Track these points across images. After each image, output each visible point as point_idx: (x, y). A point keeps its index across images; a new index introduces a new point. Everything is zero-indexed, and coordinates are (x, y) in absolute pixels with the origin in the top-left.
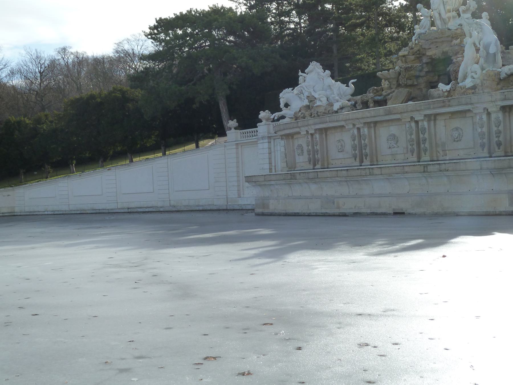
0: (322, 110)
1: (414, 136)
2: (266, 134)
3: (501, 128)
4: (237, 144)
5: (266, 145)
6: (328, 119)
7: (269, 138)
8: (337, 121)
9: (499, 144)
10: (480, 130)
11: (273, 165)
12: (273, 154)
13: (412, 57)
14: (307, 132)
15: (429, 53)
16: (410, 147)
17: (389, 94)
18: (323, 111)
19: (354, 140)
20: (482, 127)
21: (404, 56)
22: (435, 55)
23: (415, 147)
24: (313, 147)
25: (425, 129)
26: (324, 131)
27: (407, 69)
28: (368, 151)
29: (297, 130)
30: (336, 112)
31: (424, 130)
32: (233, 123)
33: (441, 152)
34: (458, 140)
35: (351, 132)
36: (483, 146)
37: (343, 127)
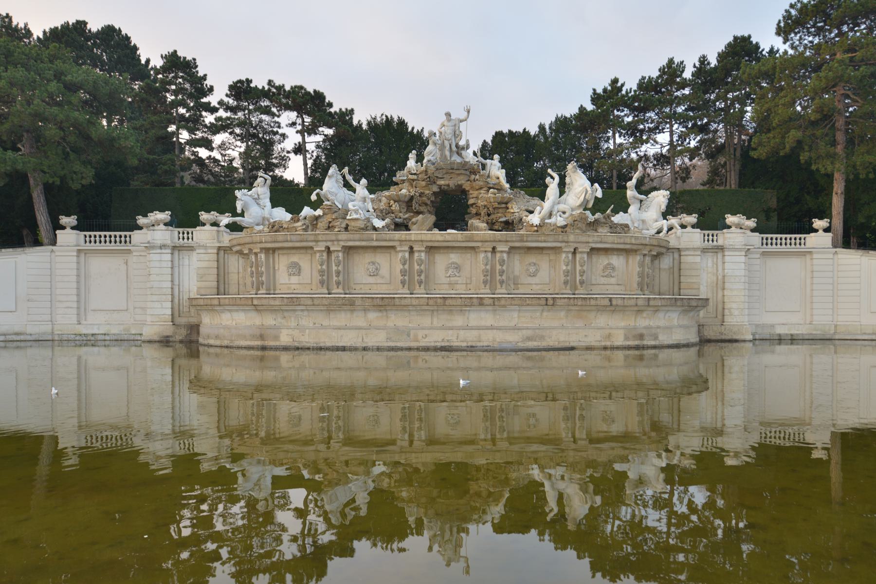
0: (361, 224)
1: (488, 267)
2: (169, 242)
3: (585, 268)
4: (79, 251)
5: (169, 257)
7: (174, 248)
8: (390, 240)
9: (582, 283)
10: (564, 268)
11: (176, 282)
12: (176, 270)
13: (424, 183)
15: (438, 183)
16: (482, 278)
18: (363, 226)
19: (404, 264)
20: (567, 265)
21: (413, 180)
22: (448, 185)
23: (489, 278)
25: (504, 261)
26: (348, 250)
28: (423, 277)
29: (311, 244)
30: (375, 229)
32: (72, 220)
33: (512, 286)
34: (534, 275)
35: (400, 255)
36: (566, 283)
37: (393, 247)
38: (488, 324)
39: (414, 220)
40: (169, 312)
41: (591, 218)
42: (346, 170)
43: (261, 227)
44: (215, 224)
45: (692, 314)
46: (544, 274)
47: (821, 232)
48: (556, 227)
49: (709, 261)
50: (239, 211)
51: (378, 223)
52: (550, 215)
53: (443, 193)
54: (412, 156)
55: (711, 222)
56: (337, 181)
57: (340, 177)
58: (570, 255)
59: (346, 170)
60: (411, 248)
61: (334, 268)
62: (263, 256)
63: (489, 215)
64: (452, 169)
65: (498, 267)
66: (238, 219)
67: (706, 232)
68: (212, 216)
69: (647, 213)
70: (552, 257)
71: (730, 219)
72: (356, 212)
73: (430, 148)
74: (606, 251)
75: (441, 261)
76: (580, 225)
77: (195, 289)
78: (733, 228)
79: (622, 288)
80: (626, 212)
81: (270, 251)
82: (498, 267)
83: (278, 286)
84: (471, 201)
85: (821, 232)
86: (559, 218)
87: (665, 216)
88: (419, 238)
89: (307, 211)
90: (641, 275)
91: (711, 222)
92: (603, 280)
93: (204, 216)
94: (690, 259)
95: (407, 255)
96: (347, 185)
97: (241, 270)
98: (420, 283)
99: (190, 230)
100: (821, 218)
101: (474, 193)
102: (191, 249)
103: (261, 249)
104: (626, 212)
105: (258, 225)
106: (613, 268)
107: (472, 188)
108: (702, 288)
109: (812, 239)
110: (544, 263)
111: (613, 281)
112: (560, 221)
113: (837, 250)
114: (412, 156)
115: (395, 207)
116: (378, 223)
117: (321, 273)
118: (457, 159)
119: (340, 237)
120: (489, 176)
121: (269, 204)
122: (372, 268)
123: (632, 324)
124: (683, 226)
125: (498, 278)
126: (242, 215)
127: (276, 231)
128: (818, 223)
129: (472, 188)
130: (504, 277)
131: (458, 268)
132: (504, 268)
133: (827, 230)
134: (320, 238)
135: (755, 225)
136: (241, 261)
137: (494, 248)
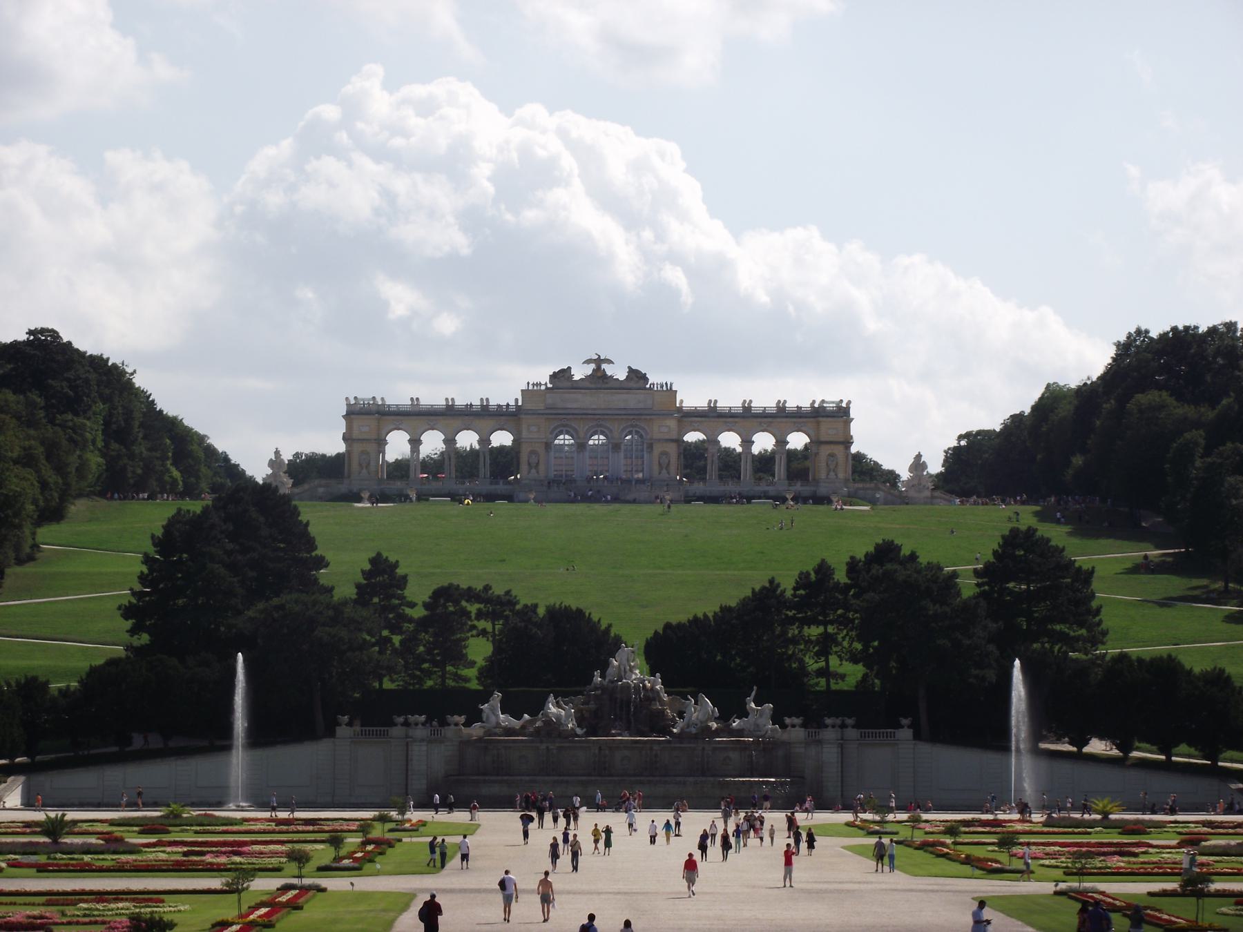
5: (424, 748)
30: (578, 736)
31: (656, 756)
40: (424, 787)
51: (579, 731)
52: (688, 726)
54: (598, 673)
55: (813, 721)
68: (456, 718)
71: (828, 721)
73: (610, 671)
87: (777, 718)
96: (558, 705)
100: (906, 718)
112: (694, 731)
114: (598, 673)
116: (579, 731)
124: (794, 726)
128: (905, 721)
133: (909, 727)
137: (651, 749)
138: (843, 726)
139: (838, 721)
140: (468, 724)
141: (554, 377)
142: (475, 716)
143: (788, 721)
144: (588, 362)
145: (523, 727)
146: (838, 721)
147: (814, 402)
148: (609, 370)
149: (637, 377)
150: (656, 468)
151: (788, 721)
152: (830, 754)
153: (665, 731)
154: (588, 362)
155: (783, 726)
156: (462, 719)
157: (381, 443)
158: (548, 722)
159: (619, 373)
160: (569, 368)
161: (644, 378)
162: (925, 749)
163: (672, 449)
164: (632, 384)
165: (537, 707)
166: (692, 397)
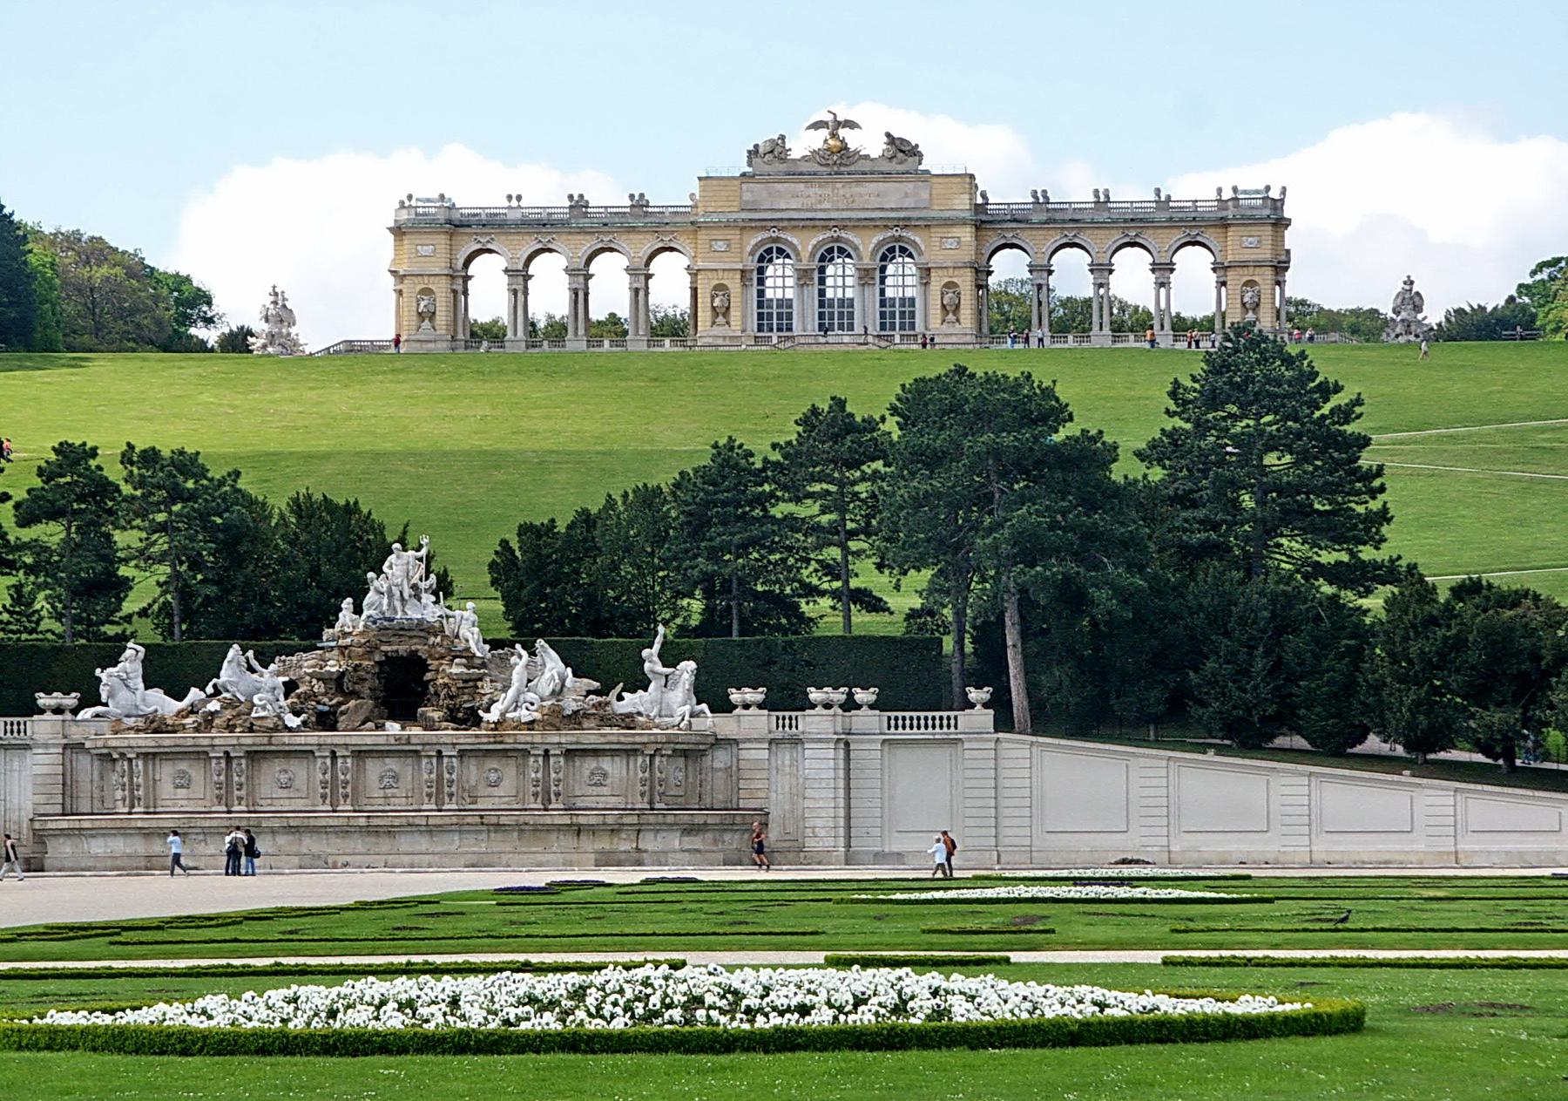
1: (433, 776)
3: (561, 775)
6: (286, 740)
14: (227, 753)
15: (384, 648)
17: (340, 704)
21: (346, 647)
24: (229, 777)
26: (254, 756)
27: (356, 668)
28: (349, 790)
30: (290, 729)
34: (495, 785)
35: (319, 761)
36: (536, 795)
37: (312, 752)
38: (423, 848)
39: (343, 708)
41: (570, 704)
42: (250, 653)
43: (131, 722)
44: (58, 710)
45: (709, 836)
46: (507, 786)
47: (979, 707)
48: (519, 725)
49: (785, 756)
50: (104, 698)
51: (293, 721)
53: (391, 661)
54: (347, 603)
55: (785, 699)
56: (239, 664)
57: (243, 659)
58: (540, 759)
59: (250, 653)
60: (333, 753)
61: (236, 779)
62: (140, 763)
63: (452, 698)
64: (402, 631)
65: (446, 776)
66: (99, 709)
67: (781, 714)
68: (56, 699)
69: (668, 698)
70: (520, 761)
71: (815, 695)
72: (264, 708)
73: (371, 597)
74: (596, 753)
75: (373, 768)
76: (551, 720)
77: (30, 807)
78: (819, 710)
79: (620, 799)
80: (646, 690)
81: (149, 756)
82: (446, 776)
83: (159, 803)
84: (428, 676)
85: (979, 707)
86: (524, 712)
87: (711, 694)
88: (342, 741)
89: (194, 694)
90: (650, 782)
91: (786, 699)
92: (590, 790)
93: (43, 700)
94: (754, 754)
95: (328, 761)
97: (96, 777)
98: (346, 796)
99: (21, 720)
101: (433, 664)
102: (27, 747)
103: (138, 755)
104: (646, 690)
105: (128, 716)
106: (605, 775)
107: (431, 656)
108: (773, 795)
109: (966, 719)
110: (509, 770)
111: (605, 790)
112: (524, 715)
113: (1001, 735)
114: (347, 603)
115: (319, 687)
117: (219, 786)
118: (414, 614)
119: (243, 741)
120: (457, 637)
121: (141, 685)
122: (283, 778)
123: (607, 847)
124: (746, 706)
125: (446, 789)
126: (106, 705)
127: (155, 731)
128: (974, 694)
129: (431, 656)
130: (454, 789)
131: (396, 778)
132: (454, 776)
133: (986, 705)
134: (217, 742)
135: (874, 697)
136: (97, 763)
138: (850, 705)
139: (839, 696)
140: (75, 711)
141: (754, 153)
142: (91, 697)
143: (735, 696)
144: (817, 125)
145: (180, 714)
146: (839, 696)
147: (1220, 191)
148: (852, 139)
149: (902, 149)
150: (935, 311)
151: (735, 696)
152: (820, 762)
153: (478, 722)
154: (817, 125)
155: (722, 706)
156: (71, 700)
157: (459, 280)
158: (230, 704)
159: (868, 142)
160: (782, 138)
161: (912, 152)
162: (1019, 749)
163: (965, 281)
164: (893, 166)
165: (206, 672)
166: (1005, 189)
